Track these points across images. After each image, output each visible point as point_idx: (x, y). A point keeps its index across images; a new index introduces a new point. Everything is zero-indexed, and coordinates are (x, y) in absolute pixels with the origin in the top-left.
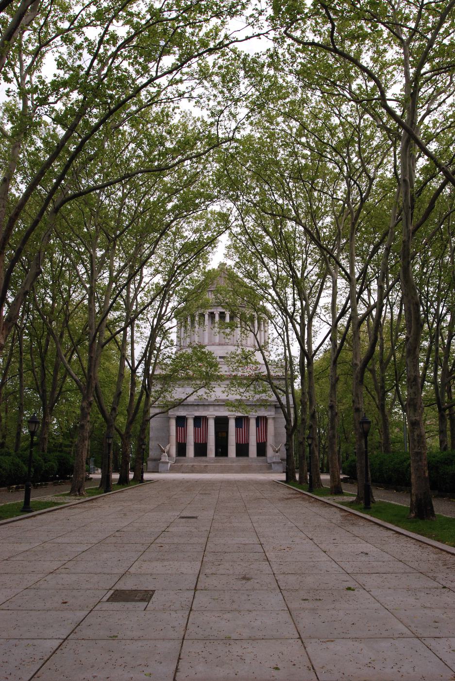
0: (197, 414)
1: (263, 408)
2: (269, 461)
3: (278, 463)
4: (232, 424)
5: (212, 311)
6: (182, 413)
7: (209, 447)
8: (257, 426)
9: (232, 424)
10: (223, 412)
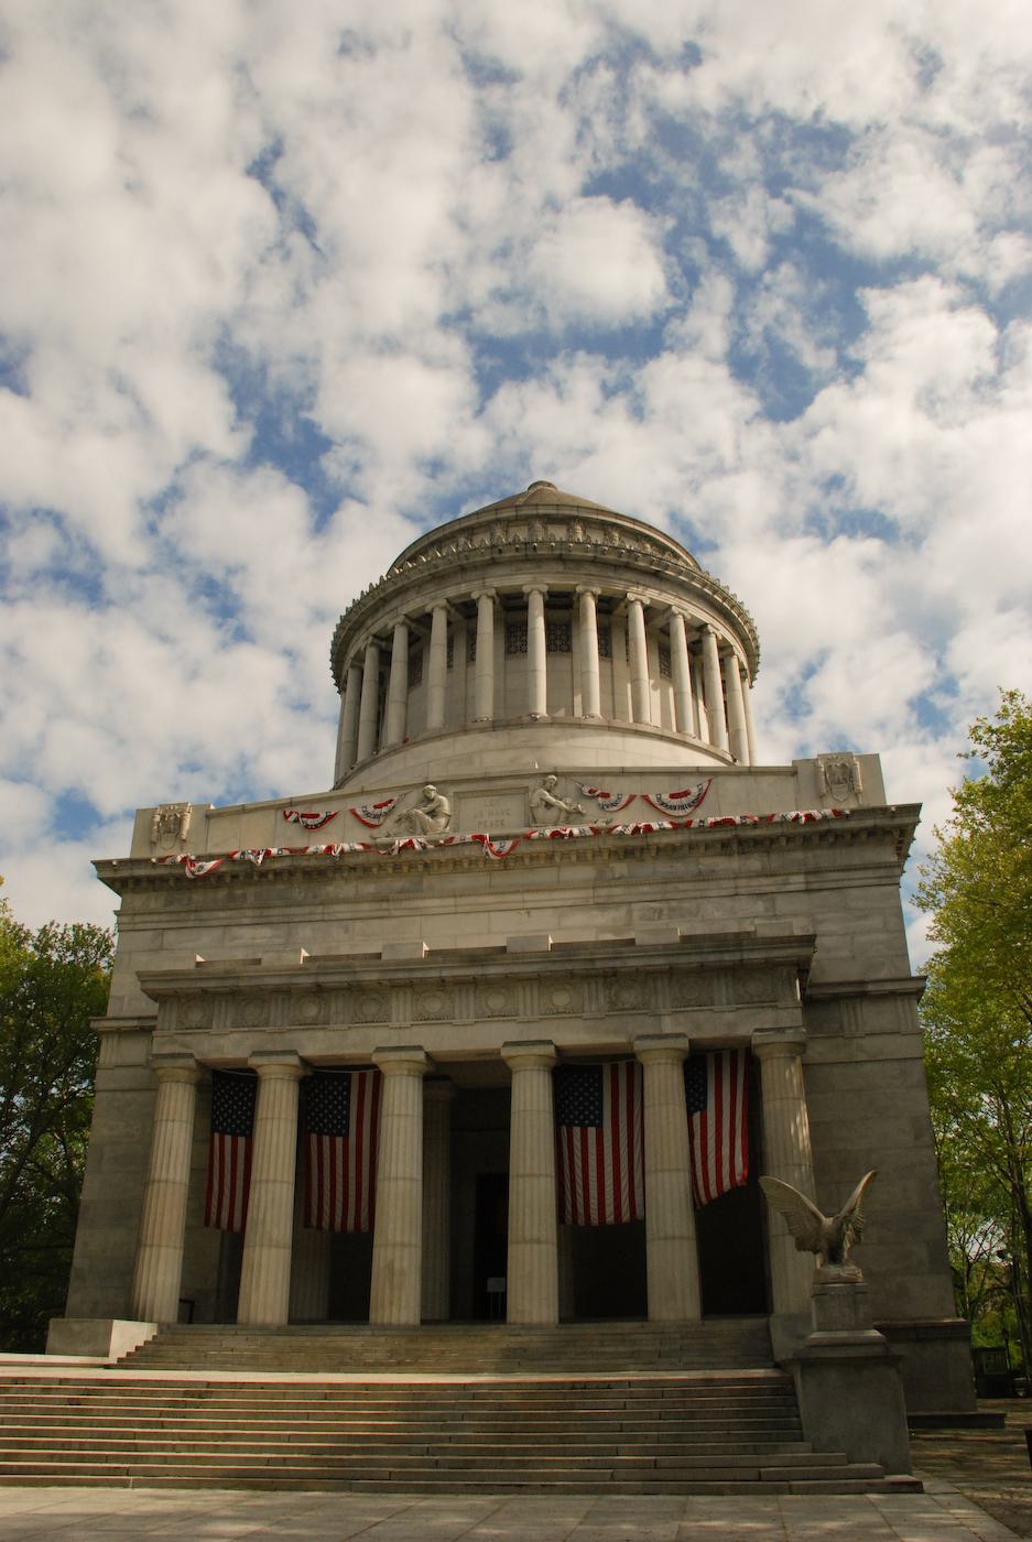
0: (318, 1045)
1: (722, 990)
2: (783, 1345)
4: (532, 1100)
5: (463, 588)
6: (229, 1045)
7: (381, 1256)
9: (532, 1100)
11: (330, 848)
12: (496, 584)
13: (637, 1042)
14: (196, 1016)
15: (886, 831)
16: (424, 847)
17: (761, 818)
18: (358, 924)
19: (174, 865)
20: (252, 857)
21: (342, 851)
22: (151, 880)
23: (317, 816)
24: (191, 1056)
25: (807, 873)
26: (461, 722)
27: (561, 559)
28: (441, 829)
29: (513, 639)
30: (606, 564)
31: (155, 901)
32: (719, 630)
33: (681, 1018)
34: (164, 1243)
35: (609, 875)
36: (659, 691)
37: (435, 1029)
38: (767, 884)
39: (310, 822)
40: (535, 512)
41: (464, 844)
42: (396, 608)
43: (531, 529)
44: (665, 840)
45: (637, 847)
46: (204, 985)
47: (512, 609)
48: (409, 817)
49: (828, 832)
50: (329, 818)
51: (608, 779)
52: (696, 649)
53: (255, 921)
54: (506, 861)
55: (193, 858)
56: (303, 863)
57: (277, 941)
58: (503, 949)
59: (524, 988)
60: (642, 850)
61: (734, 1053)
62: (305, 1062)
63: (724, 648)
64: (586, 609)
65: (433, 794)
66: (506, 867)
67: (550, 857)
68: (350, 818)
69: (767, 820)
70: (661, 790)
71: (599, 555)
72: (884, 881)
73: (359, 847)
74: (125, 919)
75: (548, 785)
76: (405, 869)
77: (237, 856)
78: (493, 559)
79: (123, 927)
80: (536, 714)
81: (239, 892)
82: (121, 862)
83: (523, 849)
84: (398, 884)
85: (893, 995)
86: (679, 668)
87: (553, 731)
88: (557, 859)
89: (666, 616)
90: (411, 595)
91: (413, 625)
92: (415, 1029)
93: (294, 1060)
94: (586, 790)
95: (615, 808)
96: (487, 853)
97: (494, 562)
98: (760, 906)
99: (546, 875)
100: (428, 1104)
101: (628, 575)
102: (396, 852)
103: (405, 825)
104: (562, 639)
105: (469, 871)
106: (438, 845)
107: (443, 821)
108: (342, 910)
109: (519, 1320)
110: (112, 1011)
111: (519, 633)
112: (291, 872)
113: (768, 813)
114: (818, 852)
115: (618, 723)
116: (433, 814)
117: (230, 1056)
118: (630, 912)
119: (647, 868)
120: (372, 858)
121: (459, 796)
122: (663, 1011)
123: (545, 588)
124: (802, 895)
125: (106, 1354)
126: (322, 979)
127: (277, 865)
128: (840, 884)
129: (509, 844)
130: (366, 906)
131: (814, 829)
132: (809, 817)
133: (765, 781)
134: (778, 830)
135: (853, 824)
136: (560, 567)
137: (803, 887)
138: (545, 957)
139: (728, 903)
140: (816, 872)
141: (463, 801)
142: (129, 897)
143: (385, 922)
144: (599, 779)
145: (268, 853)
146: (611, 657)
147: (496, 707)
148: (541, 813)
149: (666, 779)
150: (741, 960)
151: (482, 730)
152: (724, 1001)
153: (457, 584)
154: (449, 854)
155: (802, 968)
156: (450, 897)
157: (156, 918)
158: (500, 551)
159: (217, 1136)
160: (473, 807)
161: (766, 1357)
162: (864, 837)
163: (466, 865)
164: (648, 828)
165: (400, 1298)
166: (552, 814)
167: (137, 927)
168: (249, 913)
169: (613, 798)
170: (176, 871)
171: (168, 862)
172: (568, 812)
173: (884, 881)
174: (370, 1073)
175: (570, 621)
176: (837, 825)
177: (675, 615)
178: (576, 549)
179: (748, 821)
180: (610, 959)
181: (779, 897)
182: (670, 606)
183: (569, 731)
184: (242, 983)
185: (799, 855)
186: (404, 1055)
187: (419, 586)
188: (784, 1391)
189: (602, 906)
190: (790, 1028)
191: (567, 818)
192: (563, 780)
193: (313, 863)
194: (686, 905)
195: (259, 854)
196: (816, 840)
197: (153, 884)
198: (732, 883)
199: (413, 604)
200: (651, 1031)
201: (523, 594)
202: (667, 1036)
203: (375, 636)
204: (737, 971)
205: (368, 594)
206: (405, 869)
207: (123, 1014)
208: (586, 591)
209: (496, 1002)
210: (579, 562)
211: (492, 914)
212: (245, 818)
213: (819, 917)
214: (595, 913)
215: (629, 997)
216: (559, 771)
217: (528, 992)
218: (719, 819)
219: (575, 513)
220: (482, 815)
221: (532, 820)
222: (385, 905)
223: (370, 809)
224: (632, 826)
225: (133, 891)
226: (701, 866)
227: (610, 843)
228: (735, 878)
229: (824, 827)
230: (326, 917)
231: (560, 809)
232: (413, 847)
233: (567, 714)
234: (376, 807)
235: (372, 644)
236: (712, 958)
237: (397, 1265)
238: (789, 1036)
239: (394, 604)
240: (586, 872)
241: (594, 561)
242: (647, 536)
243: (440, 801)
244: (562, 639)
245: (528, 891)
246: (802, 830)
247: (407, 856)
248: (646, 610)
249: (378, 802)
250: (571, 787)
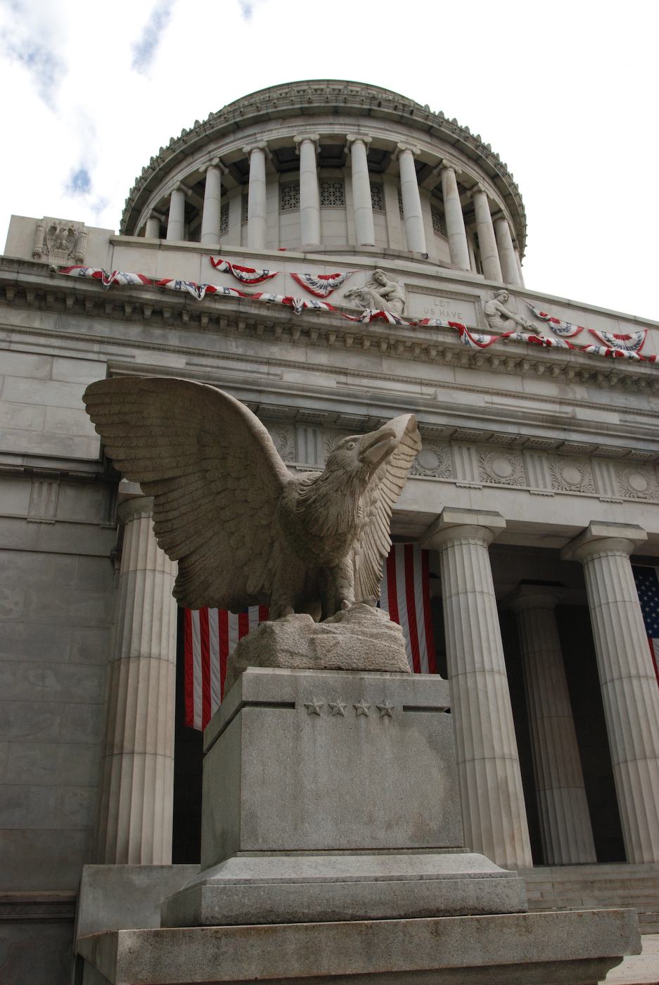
5: (337, 130)
16: (398, 322)
20: (192, 290)
21: (304, 305)
23: (253, 271)
34: (160, 751)
39: (245, 275)
41: (438, 329)
42: (255, 134)
56: (253, 311)
81: (158, 332)
92: (486, 491)
96: (467, 343)
102: (367, 320)
127: (220, 306)
136: (428, 139)
141: (411, 295)
153: (331, 124)
157: (42, 340)
167: (14, 347)
178: (446, 127)
193: (264, 312)
199: (276, 133)
209: (572, 474)
223: (315, 278)
226: (652, 405)
232: (386, 320)
234: (321, 277)
247: (378, 329)
249: (322, 274)
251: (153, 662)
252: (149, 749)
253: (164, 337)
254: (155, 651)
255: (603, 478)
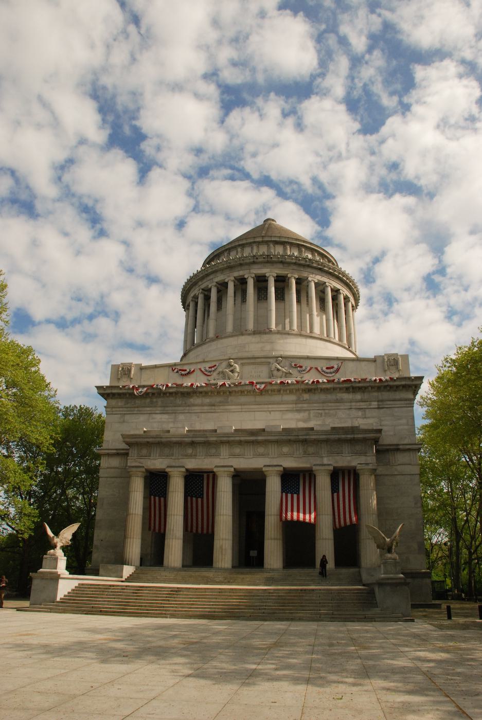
0: (192, 464)
1: (346, 448)
2: (365, 577)
3: (395, 585)
4: (273, 486)
5: (241, 273)
6: (158, 463)
7: (217, 544)
8: (334, 489)
9: (273, 486)
10: (249, 461)
11: (192, 385)
12: (255, 272)
13: (314, 467)
14: (144, 451)
15: (410, 386)
16: (230, 386)
17: (361, 379)
18: (203, 415)
19: (129, 389)
20: (161, 387)
21: (197, 386)
22: (119, 394)
23: (186, 370)
24: (143, 467)
25: (378, 401)
26: (240, 331)
27: (282, 262)
28: (236, 378)
29: (260, 294)
30: (300, 265)
31: (120, 403)
32: (345, 291)
33: (330, 458)
34: (135, 537)
35: (302, 399)
36: (319, 318)
37: (237, 459)
38: (363, 405)
40: (270, 239)
41: (246, 385)
43: (268, 246)
44: (324, 386)
45: (313, 389)
46: (148, 440)
47: (261, 282)
48: (223, 372)
49: (387, 385)
50: (189, 373)
51: (302, 360)
52: (335, 298)
53: (161, 412)
54: (262, 392)
55: (137, 386)
56: (182, 390)
57: (170, 420)
58: (264, 430)
59: (271, 445)
60: (315, 389)
61: (349, 472)
62: (187, 470)
63: (346, 299)
64: (292, 284)
65: (232, 363)
66: (261, 394)
67: (279, 391)
68: (199, 370)
69: (364, 380)
70: (323, 365)
71: (297, 261)
72: (408, 406)
73: (204, 385)
74: (108, 409)
75: (278, 362)
76: (222, 393)
77: (155, 386)
78: (254, 261)
79: (108, 413)
80: (271, 328)
81: (155, 400)
82: (107, 387)
83: (269, 387)
84: (218, 399)
85: (409, 450)
86: (329, 308)
87: (278, 336)
88: (282, 392)
89: (324, 286)
90: (219, 274)
91: (219, 286)
92: (230, 459)
93: (184, 470)
94: (293, 364)
95: (304, 372)
97: (254, 263)
98: (360, 413)
99: (277, 398)
100: (234, 485)
101: (309, 270)
102: (218, 387)
103: (221, 375)
104: (281, 295)
105: (247, 395)
106: (235, 385)
107: (236, 374)
108: (197, 409)
109: (269, 567)
110: (105, 445)
111: (263, 292)
112: (176, 393)
113: (364, 377)
114: (383, 393)
115: (303, 333)
116: (232, 371)
117: (158, 467)
118: (309, 414)
119: (316, 397)
120: (209, 389)
121: (243, 364)
122: (324, 455)
123: (276, 275)
124: (376, 410)
125: (122, 577)
126: (194, 439)
127: (171, 390)
128: (390, 406)
129: (263, 386)
130: (206, 408)
131: (382, 384)
132: (380, 380)
133: (364, 363)
134: (368, 385)
135: (397, 383)
136: (281, 266)
137: (377, 406)
138: (279, 433)
139: (347, 412)
140: (382, 401)
142: (110, 401)
143: (213, 414)
144: (298, 360)
145: (167, 386)
146: (300, 303)
147: (254, 326)
148: (275, 373)
149: (324, 361)
150: (354, 438)
151: (249, 334)
152: (347, 453)
153: (238, 271)
154: (239, 388)
155: (376, 441)
156: (239, 405)
157: (121, 409)
158: (257, 258)
159: (152, 497)
160: (248, 369)
161: (360, 582)
162: (401, 388)
163: (246, 393)
164: (318, 382)
165: (225, 558)
166: (280, 374)
167: (114, 413)
168: (159, 409)
169: (304, 368)
170: (129, 391)
171: (126, 387)
172: (286, 373)
173: (408, 406)
174: (211, 475)
175: (284, 287)
176: (391, 383)
177: (327, 286)
179: (357, 380)
180: (304, 435)
181: (367, 410)
182: (325, 283)
183: (284, 336)
184: (163, 440)
185: (375, 394)
186: (226, 469)
187: (222, 270)
188: (371, 593)
189: (299, 411)
190: (371, 463)
191: (285, 375)
192: (284, 360)
193: (185, 390)
194: (331, 412)
195: (164, 386)
196: (382, 388)
197: (120, 396)
198: (349, 404)
199: (220, 278)
200: (318, 463)
201: (266, 276)
202: (325, 465)
203: (202, 289)
204: (352, 442)
205: (200, 272)
206: (222, 393)
207: (110, 448)
208: (292, 276)
209: (261, 450)
210: (289, 264)
211: (256, 412)
212: (156, 370)
213: (383, 418)
214: (296, 413)
215: (311, 450)
216: (283, 356)
217: (273, 446)
218: (345, 379)
219: (286, 240)
220: (251, 372)
221: (271, 375)
222: (213, 408)
223: (207, 369)
224: (311, 381)
225: (112, 398)
227: (303, 387)
228: (351, 402)
229: (386, 384)
230: (190, 411)
231: (283, 372)
233: (282, 328)
234: (209, 368)
235: (202, 293)
236: (343, 436)
237: (224, 547)
238: (370, 467)
239: (211, 277)
240: (293, 397)
241: (295, 264)
242: (316, 250)
243: (235, 366)
244: (281, 295)
245: (270, 404)
246: (377, 385)
248: (316, 284)
250: (287, 364)
251: (134, 516)
252: (132, 537)
253: (157, 402)
254: (134, 512)
255: (272, 449)
